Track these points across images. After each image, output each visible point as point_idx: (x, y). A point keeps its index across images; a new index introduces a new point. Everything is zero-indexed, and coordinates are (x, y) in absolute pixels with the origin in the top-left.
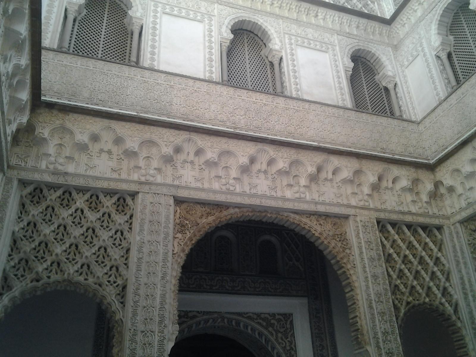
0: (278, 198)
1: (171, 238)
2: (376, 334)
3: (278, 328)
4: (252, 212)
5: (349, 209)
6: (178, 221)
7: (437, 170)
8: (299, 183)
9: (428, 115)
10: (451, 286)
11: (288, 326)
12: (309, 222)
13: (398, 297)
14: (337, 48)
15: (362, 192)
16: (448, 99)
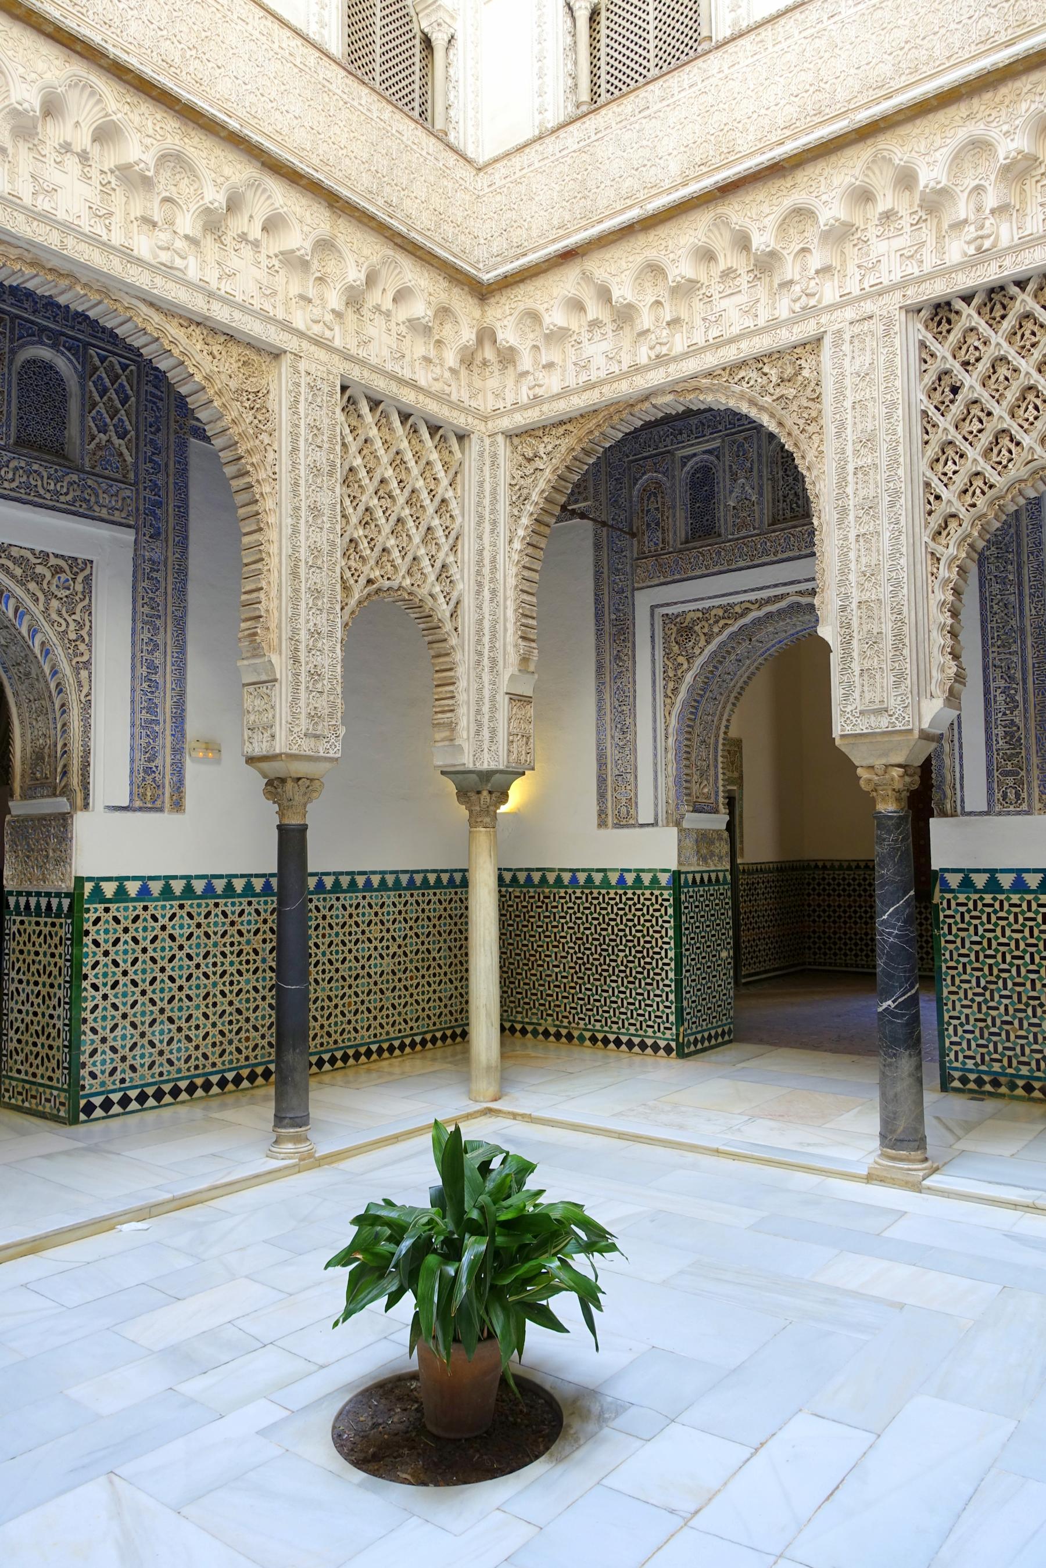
0: (114, 248)
2: (295, 631)
3: (53, 588)
4: (32, 264)
5: (285, 336)
7: (492, 300)
8: (173, 224)
9: (507, 155)
11: (79, 588)
12: (184, 340)
13: (352, 563)
16: (561, 133)
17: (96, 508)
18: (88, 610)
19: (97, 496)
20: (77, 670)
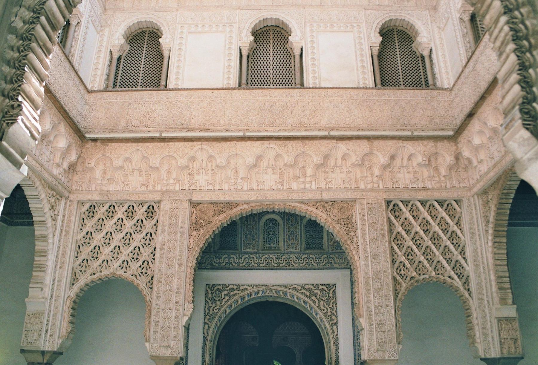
1: (186, 236)
6: (194, 221)
10: (464, 258)
11: (331, 295)
13: (402, 272)
14: (364, 24)
15: (372, 174)
17: (335, 265)
18: (335, 303)
19: (334, 260)
20: (332, 326)
